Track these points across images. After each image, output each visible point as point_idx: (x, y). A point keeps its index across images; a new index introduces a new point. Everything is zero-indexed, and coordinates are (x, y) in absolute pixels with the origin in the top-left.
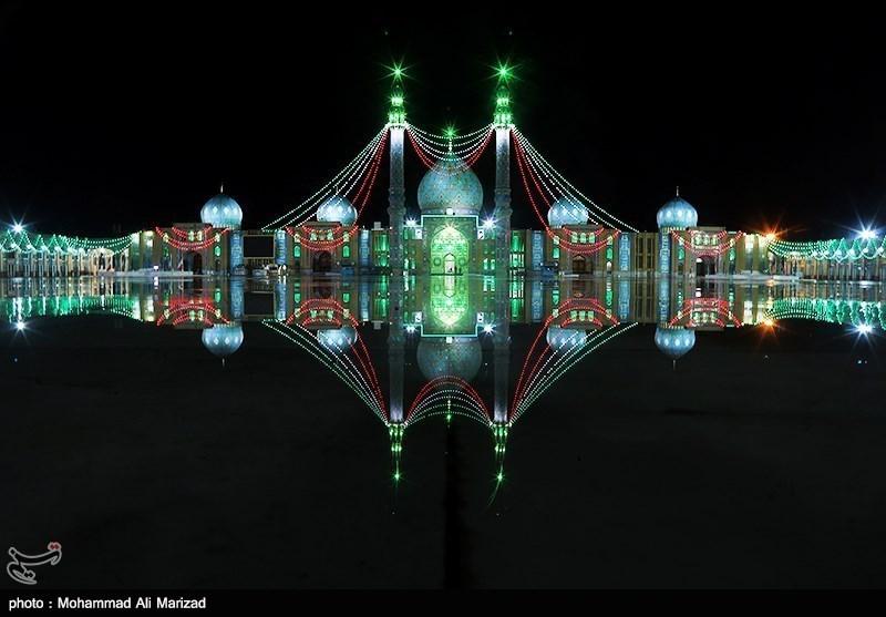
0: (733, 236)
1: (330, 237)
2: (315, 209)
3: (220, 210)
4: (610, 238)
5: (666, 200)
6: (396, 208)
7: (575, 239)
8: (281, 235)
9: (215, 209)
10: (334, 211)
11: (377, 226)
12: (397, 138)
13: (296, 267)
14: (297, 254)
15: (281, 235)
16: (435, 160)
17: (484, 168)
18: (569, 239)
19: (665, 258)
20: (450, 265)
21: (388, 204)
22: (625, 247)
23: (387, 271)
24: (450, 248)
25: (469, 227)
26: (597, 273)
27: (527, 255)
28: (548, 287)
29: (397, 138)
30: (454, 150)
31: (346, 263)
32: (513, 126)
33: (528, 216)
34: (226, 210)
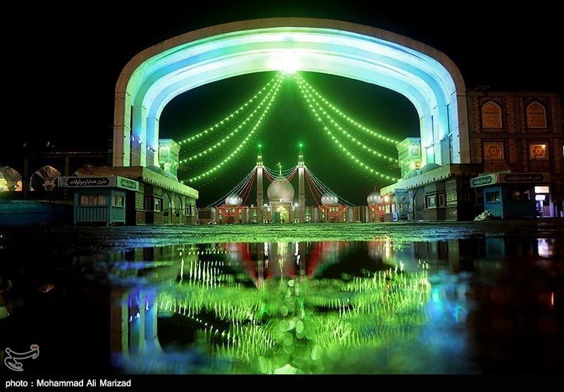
2: (226, 197)
6: (260, 200)
8: (214, 210)
10: (233, 200)
11: (252, 206)
12: (260, 171)
15: (214, 210)
17: (294, 181)
18: (328, 210)
29: (260, 171)
32: (305, 166)
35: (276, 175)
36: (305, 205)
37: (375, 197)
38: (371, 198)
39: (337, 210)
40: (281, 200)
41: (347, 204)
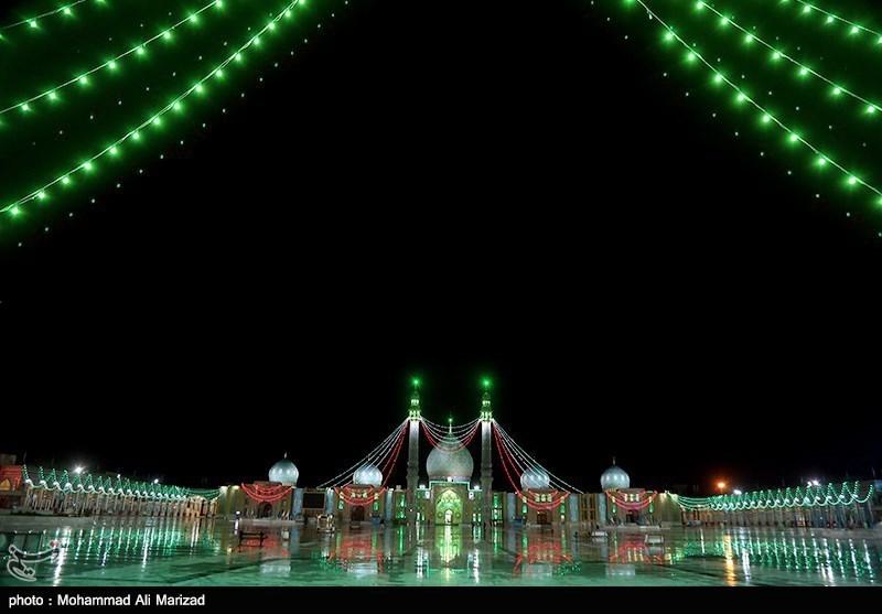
0: (651, 495)
1: (365, 495)
2: (354, 471)
3: (284, 471)
4: (563, 498)
5: (606, 467)
7: (538, 500)
8: (330, 491)
9: (281, 471)
10: (369, 476)
11: (399, 488)
12: (415, 426)
13: (339, 516)
14: (341, 507)
15: (330, 491)
16: (438, 441)
17: (474, 446)
19: (603, 513)
20: (448, 517)
21: (406, 473)
22: (574, 507)
23: (404, 523)
24: (449, 505)
25: (461, 490)
26: (554, 524)
27: (503, 510)
28: (519, 537)
29: (415, 426)
30: (453, 430)
31: (376, 515)
32: (493, 420)
33: (505, 480)
34: (288, 472)
35: (444, 435)
36: (493, 489)
37: (616, 477)
38: (608, 478)
39: (550, 499)
40: (449, 479)
41: (566, 487)
